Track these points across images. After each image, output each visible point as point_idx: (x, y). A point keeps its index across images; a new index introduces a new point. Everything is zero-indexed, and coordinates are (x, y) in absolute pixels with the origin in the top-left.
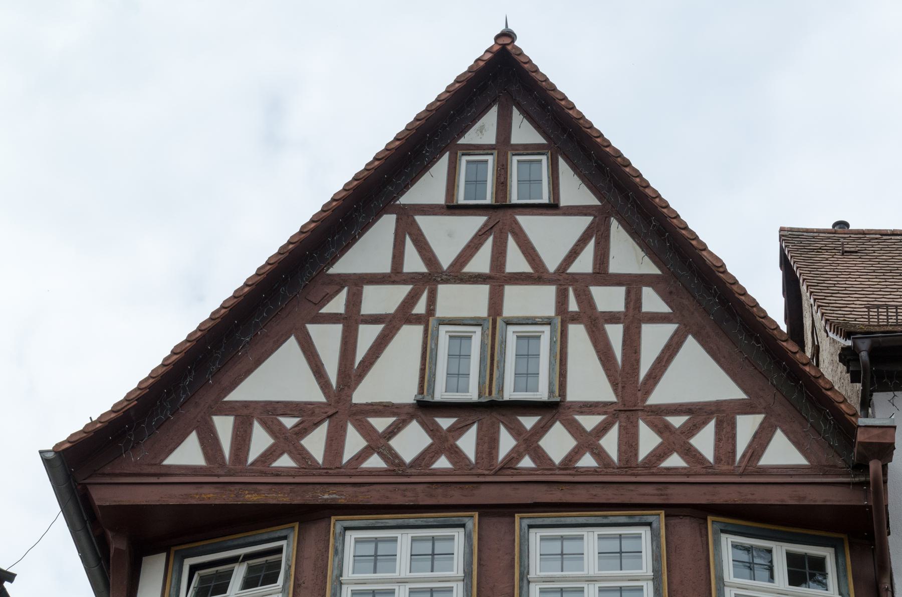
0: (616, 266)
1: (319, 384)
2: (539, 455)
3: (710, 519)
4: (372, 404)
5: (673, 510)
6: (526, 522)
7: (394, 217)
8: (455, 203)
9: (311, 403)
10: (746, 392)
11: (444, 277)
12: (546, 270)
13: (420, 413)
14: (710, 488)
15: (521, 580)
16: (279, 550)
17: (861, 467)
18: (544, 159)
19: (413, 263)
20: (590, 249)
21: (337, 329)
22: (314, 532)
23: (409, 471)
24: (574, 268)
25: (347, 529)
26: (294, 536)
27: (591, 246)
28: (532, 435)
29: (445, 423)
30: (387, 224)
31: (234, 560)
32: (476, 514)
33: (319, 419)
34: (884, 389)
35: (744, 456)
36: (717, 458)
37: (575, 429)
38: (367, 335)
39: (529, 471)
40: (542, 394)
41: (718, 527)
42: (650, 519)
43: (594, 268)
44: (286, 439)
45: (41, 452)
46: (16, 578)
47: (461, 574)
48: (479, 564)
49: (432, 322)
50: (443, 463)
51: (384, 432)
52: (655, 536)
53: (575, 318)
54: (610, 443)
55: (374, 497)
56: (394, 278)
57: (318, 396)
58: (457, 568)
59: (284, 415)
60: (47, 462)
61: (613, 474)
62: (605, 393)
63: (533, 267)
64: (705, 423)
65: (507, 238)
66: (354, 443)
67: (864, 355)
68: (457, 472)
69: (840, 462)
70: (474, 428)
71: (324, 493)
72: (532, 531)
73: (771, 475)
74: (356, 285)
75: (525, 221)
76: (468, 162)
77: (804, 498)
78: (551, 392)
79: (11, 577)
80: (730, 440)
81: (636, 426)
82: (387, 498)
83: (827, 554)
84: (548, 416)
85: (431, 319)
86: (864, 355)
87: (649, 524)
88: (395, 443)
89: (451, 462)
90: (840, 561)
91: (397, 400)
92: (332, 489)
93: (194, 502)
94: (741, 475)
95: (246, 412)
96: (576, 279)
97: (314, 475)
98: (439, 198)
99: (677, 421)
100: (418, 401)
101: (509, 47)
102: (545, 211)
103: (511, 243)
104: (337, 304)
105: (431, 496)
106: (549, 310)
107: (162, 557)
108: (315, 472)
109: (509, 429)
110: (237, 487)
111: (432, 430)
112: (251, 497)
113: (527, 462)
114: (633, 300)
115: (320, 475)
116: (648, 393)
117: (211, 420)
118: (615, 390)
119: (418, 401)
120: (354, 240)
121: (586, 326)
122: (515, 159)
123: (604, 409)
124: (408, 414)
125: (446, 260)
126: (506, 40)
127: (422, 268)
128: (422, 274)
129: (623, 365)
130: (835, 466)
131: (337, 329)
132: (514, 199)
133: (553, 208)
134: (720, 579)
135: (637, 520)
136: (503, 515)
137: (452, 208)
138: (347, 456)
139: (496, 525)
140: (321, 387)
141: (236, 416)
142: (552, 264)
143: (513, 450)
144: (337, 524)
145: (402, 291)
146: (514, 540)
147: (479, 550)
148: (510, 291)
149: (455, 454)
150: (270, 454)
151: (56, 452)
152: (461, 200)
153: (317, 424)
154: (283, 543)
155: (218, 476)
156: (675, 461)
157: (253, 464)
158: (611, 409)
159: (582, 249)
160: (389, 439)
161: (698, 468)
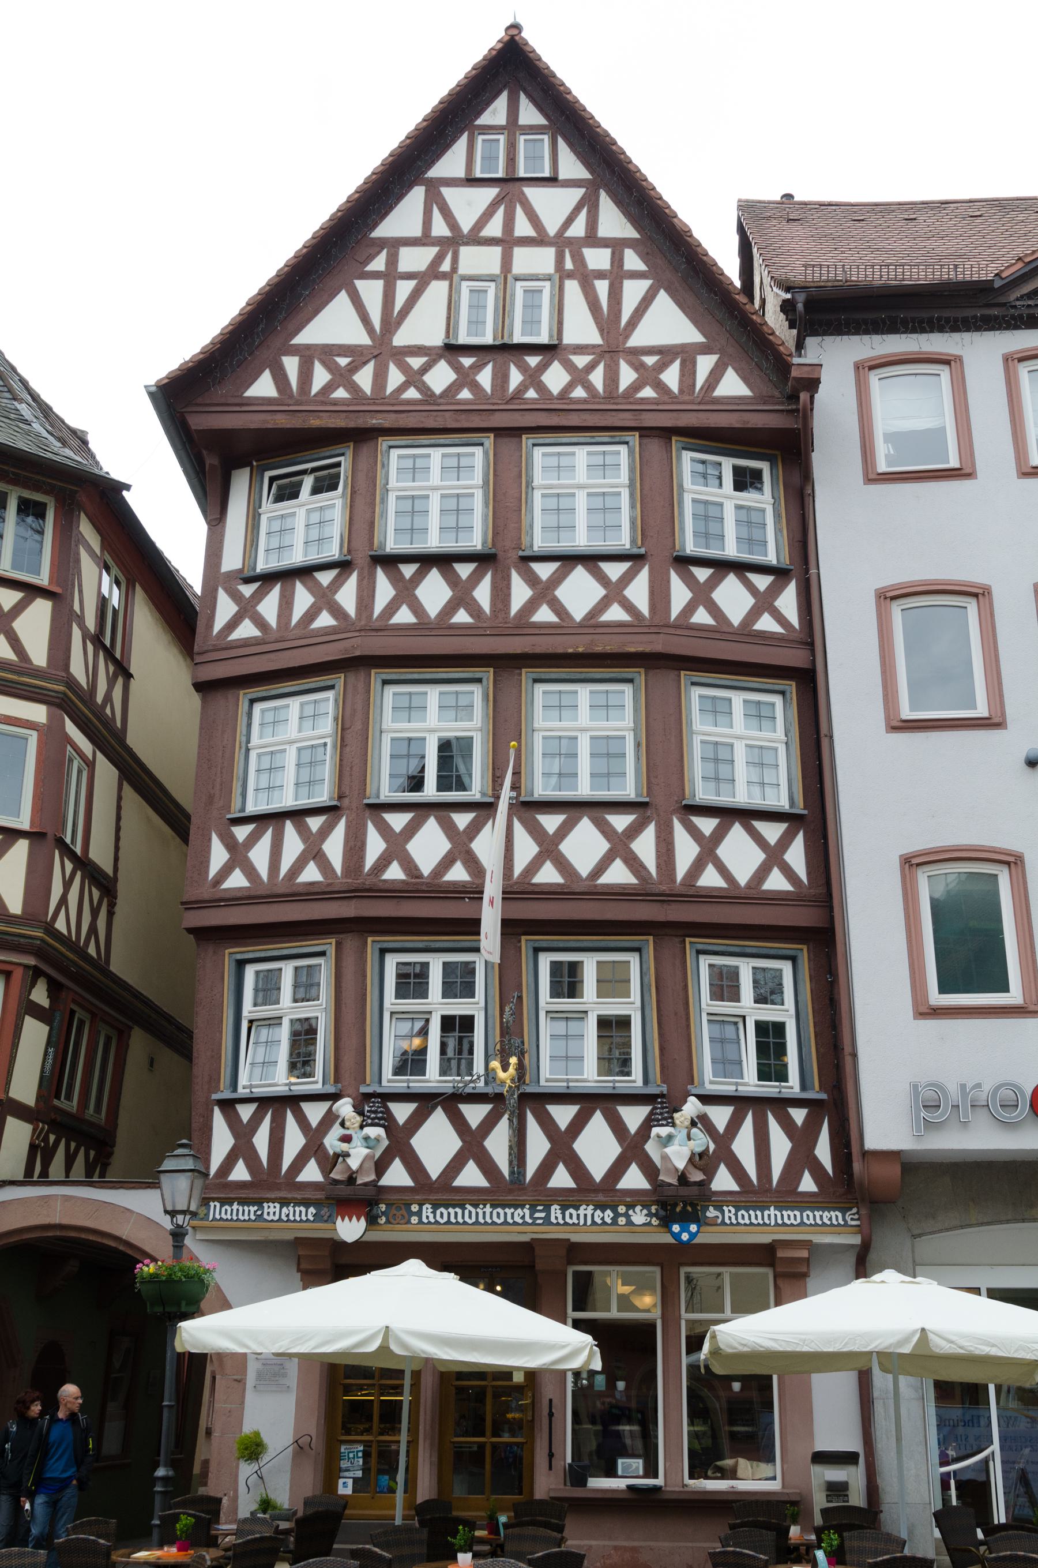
0: (603, 232)
1: (366, 329)
2: (541, 388)
3: (674, 439)
4: (409, 347)
5: (645, 432)
6: (531, 442)
7: (423, 188)
8: (473, 177)
9: (360, 346)
10: (705, 336)
11: (465, 240)
12: (547, 234)
13: (447, 354)
14: (675, 414)
15: (527, 487)
16: (338, 465)
17: (794, 397)
18: (546, 138)
19: (440, 228)
20: (583, 216)
21: (379, 285)
22: (365, 450)
24: (569, 233)
25: (391, 447)
26: (349, 453)
27: (584, 213)
28: (536, 372)
29: (467, 361)
30: (417, 195)
31: (304, 472)
32: (492, 435)
33: (367, 358)
34: (815, 333)
35: (702, 388)
36: (681, 390)
37: (569, 366)
38: (404, 289)
39: (533, 401)
40: (543, 338)
41: (680, 445)
42: (627, 439)
43: (586, 233)
44: (341, 375)
45: (146, 387)
46: (132, 488)
47: (481, 482)
48: (495, 475)
49: (455, 277)
50: (465, 394)
51: (419, 369)
52: (631, 453)
53: (570, 275)
54: (597, 379)
55: (412, 422)
56: (424, 241)
57: (364, 340)
58: (478, 478)
59: (339, 355)
60: (152, 395)
61: (599, 403)
62: (593, 337)
63: (537, 232)
64: (672, 362)
65: (515, 207)
66: (395, 378)
67: (800, 306)
68: (477, 402)
69: (777, 394)
70: (490, 367)
71: (372, 418)
72: (536, 448)
73: (722, 404)
74: (394, 247)
75: (531, 193)
76: (484, 141)
77: (748, 422)
78: (551, 336)
79: (128, 487)
80: (692, 376)
81: (618, 365)
82: (422, 422)
83: (764, 466)
84: (549, 356)
85: (455, 276)
86: (800, 306)
87: (627, 443)
88: (427, 378)
89: (472, 394)
90: (774, 471)
91: (428, 343)
92: (379, 415)
93: (270, 426)
94: (699, 403)
95: (308, 353)
96: (571, 242)
97: (364, 404)
98: (461, 173)
99: (650, 360)
100: (445, 344)
101: (517, 38)
102: (546, 183)
103: (519, 212)
104: (379, 264)
105: (457, 421)
106: (549, 267)
107: (248, 470)
108: (364, 402)
109: (518, 367)
110: (304, 414)
111: (457, 368)
112: (315, 422)
113: (531, 394)
114: (617, 260)
115: (369, 404)
116: (627, 337)
117: (281, 359)
118: (602, 335)
119: (445, 344)
120: (391, 208)
121: (579, 282)
122: (523, 138)
123: (593, 350)
124: (437, 354)
125: (466, 225)
127: (446, 232)
128: (447, 238)
129: (608, 314)
130: (774, 397)
131: (379, 285)
132: (522, 173)
133: (552, 180)
134: (681, 486)
135: (617, 439)
136: (514, 436)
137: (471, 181)
138: (389, 390)
139: (507, 444)
140: (368, 333)
141: (301, 356)
142: (552, 230)
143: (522, 384)
144: (383, 443)
145: (432, 251)
146: (521, 456)
147: (495, 464)
148: (519, 252)
149: (475, 387)
150: (329, 388)
151: (157, 387)
152: (478, 174)
153: (365, 363)
154: (341, 459)
155: (289, 405)
156: (648, 392)
157: (315, 395)
158: (598, 350)
159: (576, 216)
160: (423, 375)
161: (666, 398)
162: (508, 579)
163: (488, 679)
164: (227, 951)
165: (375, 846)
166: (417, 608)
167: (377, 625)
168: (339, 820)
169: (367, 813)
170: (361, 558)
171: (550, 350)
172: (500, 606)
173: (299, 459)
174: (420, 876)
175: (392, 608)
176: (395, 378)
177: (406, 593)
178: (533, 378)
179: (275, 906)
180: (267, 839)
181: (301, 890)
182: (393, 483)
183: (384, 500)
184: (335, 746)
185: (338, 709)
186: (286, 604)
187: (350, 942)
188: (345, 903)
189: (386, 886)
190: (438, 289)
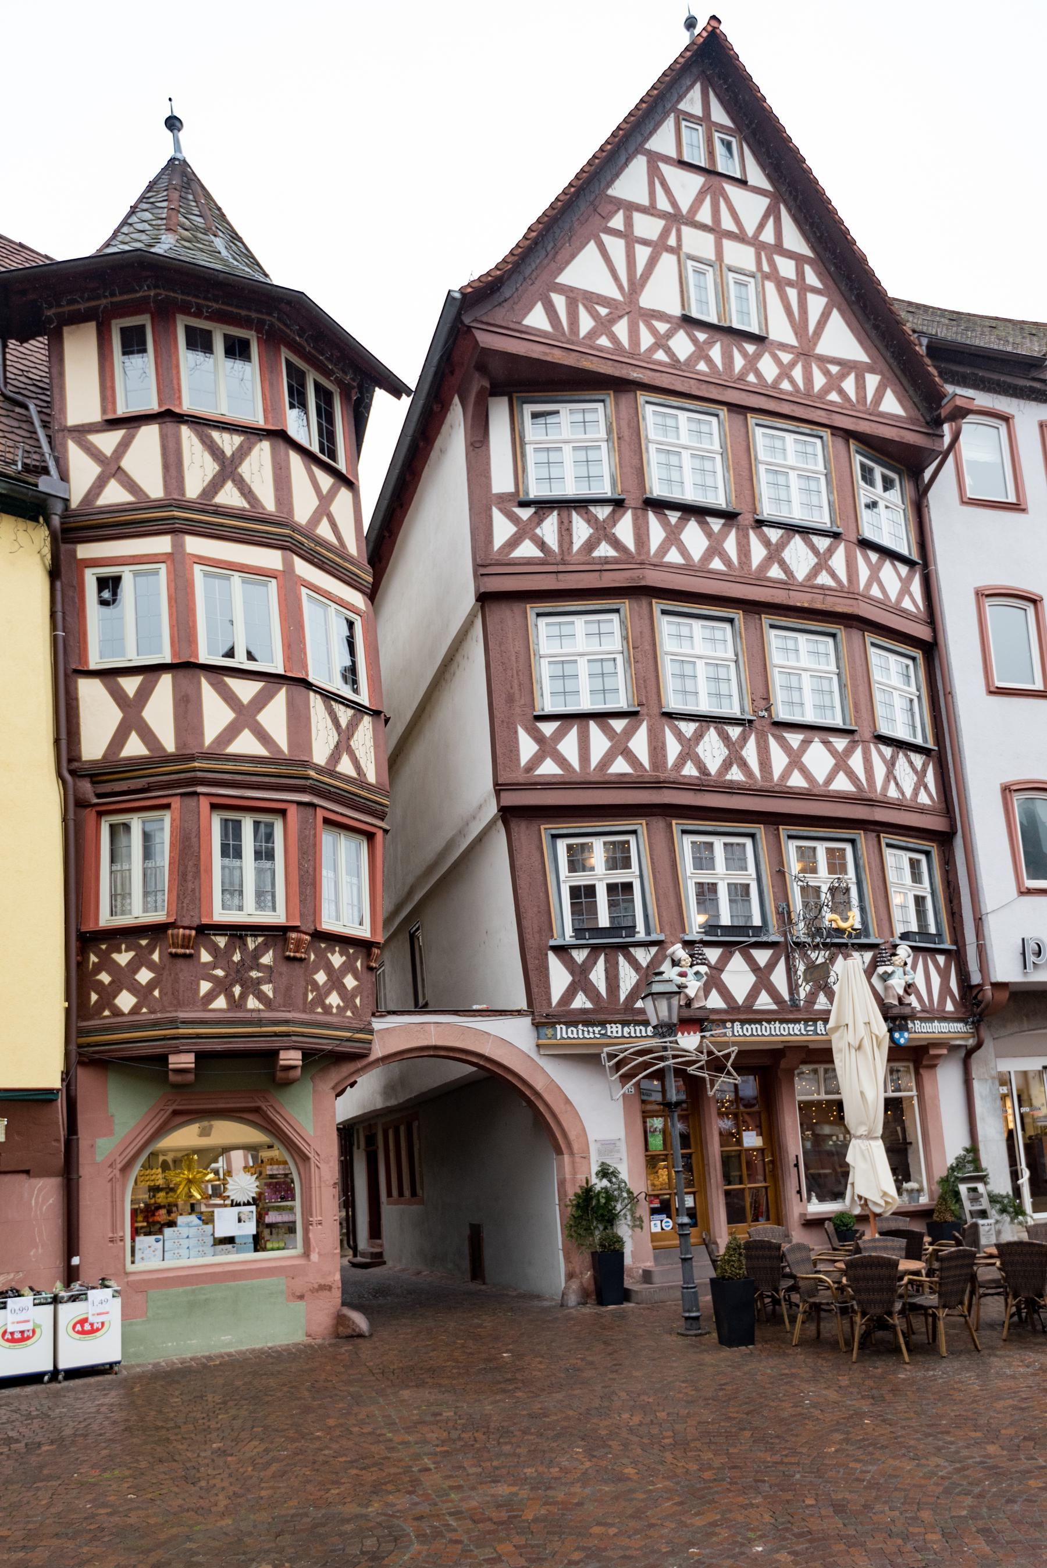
13: (684, 325)
23: (683, 367)
105: (699, 389)
119: (683, 315)
126: (714, 23)
143: (744, 367)
144: (642, 397)
149: (709, 361)
162: (747, 536)
163: (739, 619)
164: (542, 827)
165: (673, 749)
166: (684, 551)
167: (655, 561)
168: (641, 723)
169: (664, 720)
170: (633, 499)
171: (759, 339)
172: (744, 559)
173: (559, 398)
174: (709, 774)
175: (663, 549)
176: (646, 340)
177: (673, 537)
178: (752, 363)
179: (590, 791)
180: (574, 733)
181: (613, 779)
182: (652, 436)
183: (647, 449)
184: (627, 661)
185: (627, 629)
186: (565, 531)
187: (659, 824)
188: (655, 791)
189: (686, 781)
190: (668, 262)
